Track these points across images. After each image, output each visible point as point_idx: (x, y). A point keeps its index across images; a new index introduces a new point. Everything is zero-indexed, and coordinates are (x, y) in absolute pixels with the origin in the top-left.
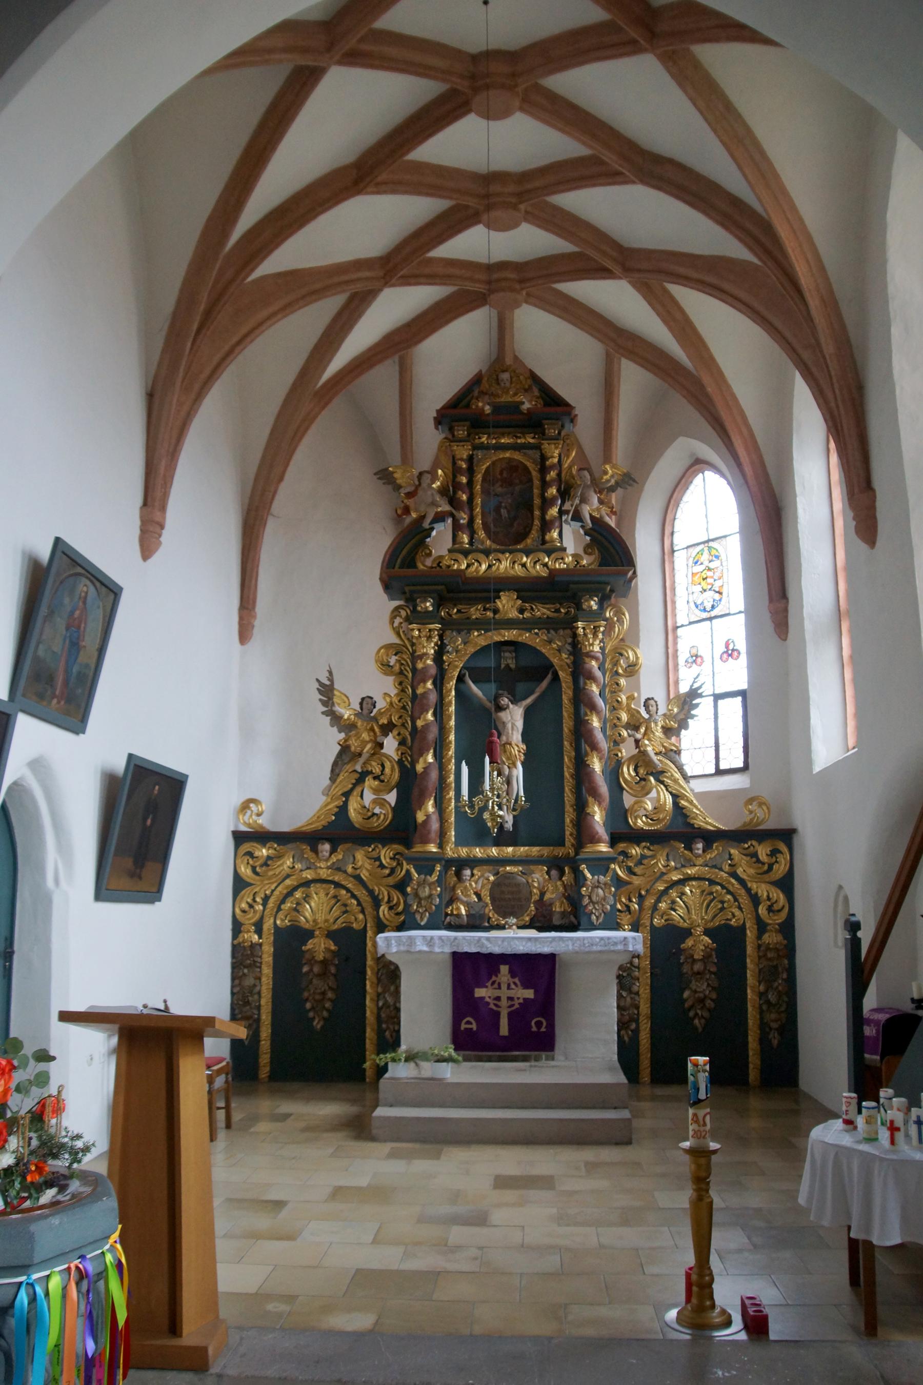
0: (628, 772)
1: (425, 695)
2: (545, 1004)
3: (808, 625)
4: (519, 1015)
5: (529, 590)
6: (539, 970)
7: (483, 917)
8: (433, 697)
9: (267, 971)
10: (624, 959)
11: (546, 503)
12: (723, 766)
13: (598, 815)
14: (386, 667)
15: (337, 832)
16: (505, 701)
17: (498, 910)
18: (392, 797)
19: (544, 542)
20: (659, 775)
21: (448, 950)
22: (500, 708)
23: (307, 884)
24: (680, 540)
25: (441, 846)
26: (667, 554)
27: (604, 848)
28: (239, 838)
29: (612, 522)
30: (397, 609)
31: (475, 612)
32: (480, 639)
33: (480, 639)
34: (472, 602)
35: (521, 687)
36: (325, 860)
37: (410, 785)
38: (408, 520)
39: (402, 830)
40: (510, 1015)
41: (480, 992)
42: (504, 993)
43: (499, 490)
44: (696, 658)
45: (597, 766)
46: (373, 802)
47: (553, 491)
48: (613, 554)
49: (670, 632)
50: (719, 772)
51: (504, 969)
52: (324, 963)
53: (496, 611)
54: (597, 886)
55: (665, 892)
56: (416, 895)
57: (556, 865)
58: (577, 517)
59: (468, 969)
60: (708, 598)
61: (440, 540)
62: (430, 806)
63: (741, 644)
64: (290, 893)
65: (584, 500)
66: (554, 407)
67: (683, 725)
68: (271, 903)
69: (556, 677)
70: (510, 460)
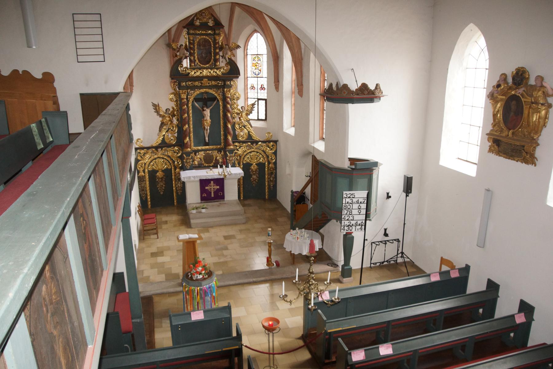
0: (237, 126)
1: (184, 109)
2: (222, 189)
3: (284, 94)
4: (216, 192)
5: (211, 78)
6: (220, 182)
7: (202, 164)
8: (187, 110)
9: (148, 183)
10: (239, 177)
11: (216, 54)
12: (260, 118)
13: (230, 138)
14: (171, 100)
15: (164, 145)
16: (205, 109)
17: (205, 162)
18: (176, 135)
19: (215, 65)
20: (245, 126)
21: (198, 179)
22: (204, 110)
23: (155, 159)
24: (250, 52)
25: (190, 148)
26: (246, 55)
27: (232, 147)
28: (136, 149)
29: (233, 58)
30: (175, 82)
31: (197, 83)
32: (198, 92)
33: (198, 92)
34: (195, 81)
35: (209, 103)
36: (160, 152)
37: (182, 135)
38: (177, 58)
39: (180, 143)
40: (214, 192)
41: (206, 188)
42: (212, 187)
43: (202, 48)
44: (253, 88)
45: (229, 126)
46: (171, 137)
47: (218, 51)
48: (234, 71)
49: (246, 78)
50: (258, 120)
51: (212, 182)
52: (162, 178)
53: (202, 83)
54: (230, 157)
55: (246, 155)
56: (186, 162)
57: (219, 150)
58: (225, 58)
59: (204, 183)
60: (257, 71)
61: (186, 63)
62: (188, 139)
63: (266, 87)
64: (151, 162)
65: (226, 54)
66: (218, 25)
67: (251, 112)
68: (147, 166)
69: (218, 100)
70: (205, 39)
